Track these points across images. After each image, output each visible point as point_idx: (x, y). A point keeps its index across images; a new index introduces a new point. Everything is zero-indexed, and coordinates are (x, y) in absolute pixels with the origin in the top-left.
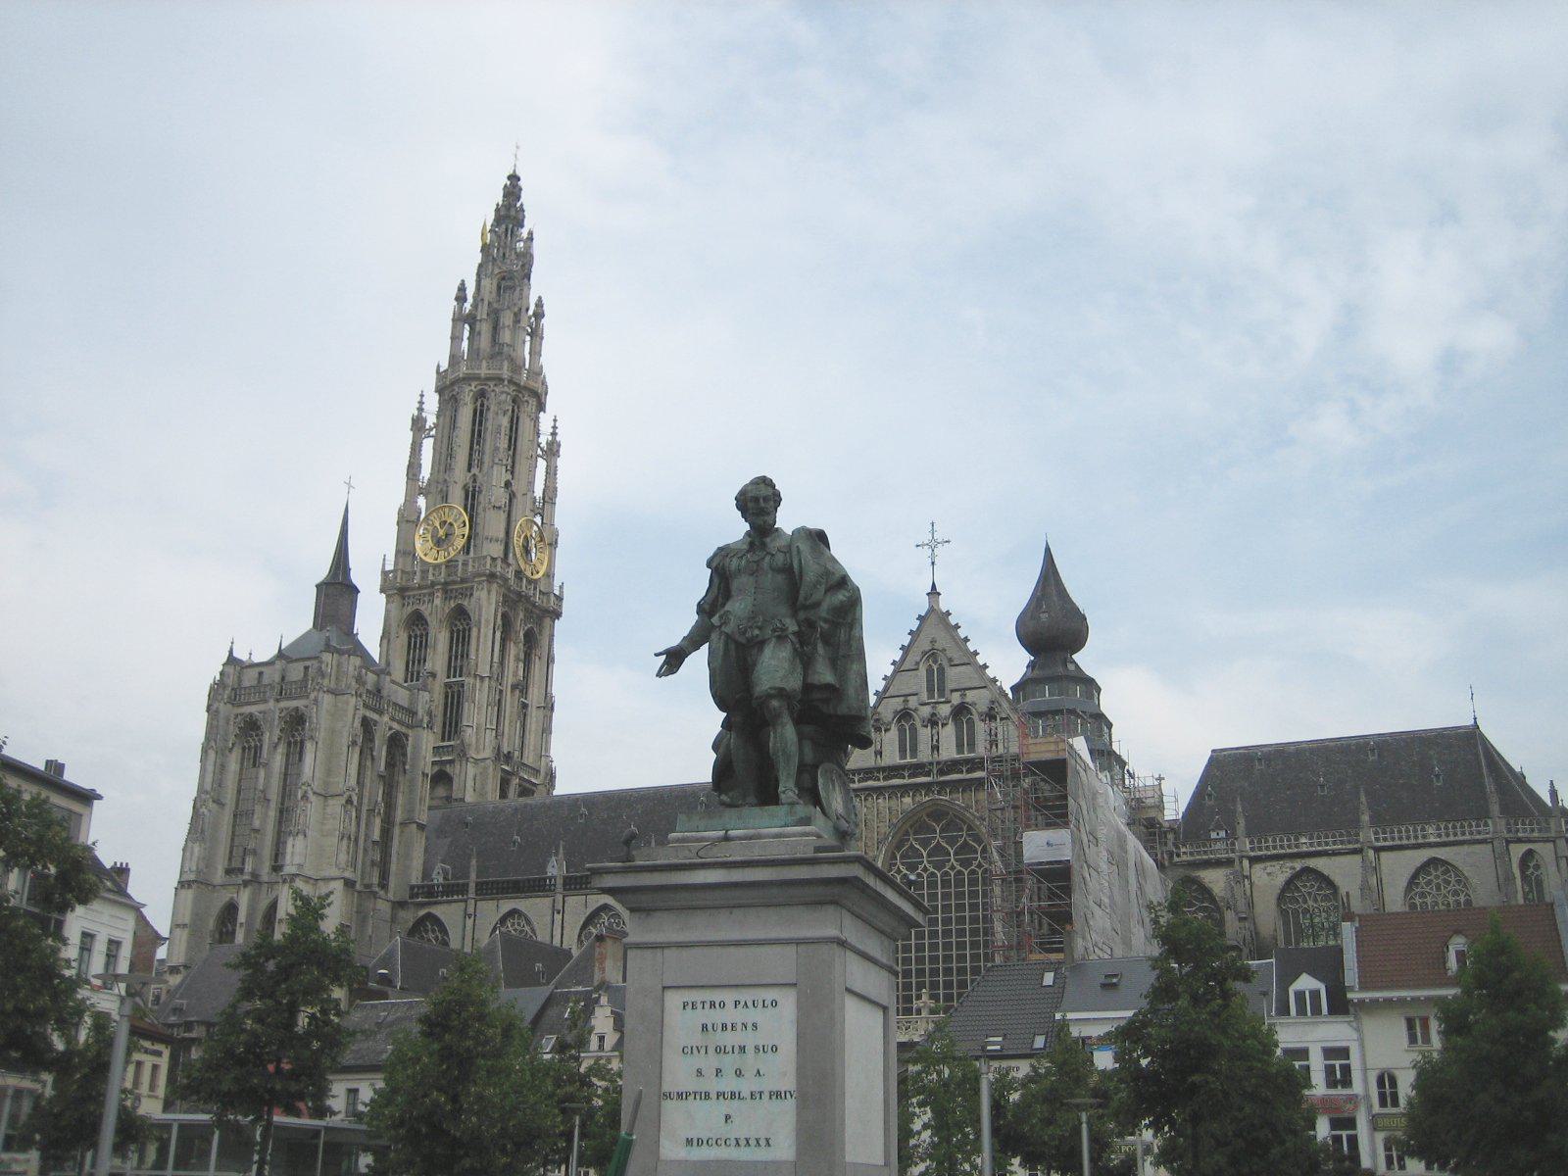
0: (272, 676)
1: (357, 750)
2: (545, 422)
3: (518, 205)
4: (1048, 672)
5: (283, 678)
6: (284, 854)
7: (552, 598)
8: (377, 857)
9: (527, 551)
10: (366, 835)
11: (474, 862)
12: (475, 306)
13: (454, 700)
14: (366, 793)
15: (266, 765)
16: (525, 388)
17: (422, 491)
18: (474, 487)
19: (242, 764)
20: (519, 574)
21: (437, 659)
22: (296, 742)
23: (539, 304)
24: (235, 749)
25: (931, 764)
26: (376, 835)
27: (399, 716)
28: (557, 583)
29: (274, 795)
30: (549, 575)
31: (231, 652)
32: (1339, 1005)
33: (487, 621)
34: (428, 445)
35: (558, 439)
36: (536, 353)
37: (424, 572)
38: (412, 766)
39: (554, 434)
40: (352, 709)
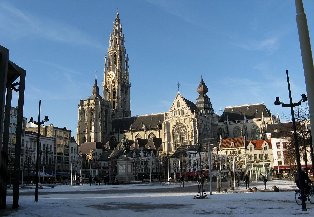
2: (126, 56)
6: (92, 129)
8: (105, 128)
9: (124, 77)
10: (103, 125)
11: (119, 128)
14: (103, 119)
16: (122, 51)
20: (123, 81)
23: (123, 36)
26: (105, 125)
28: (129, 82)
30: (128, 81)
32: (218, 150)
36: (123, 44)
39: (127, 57)
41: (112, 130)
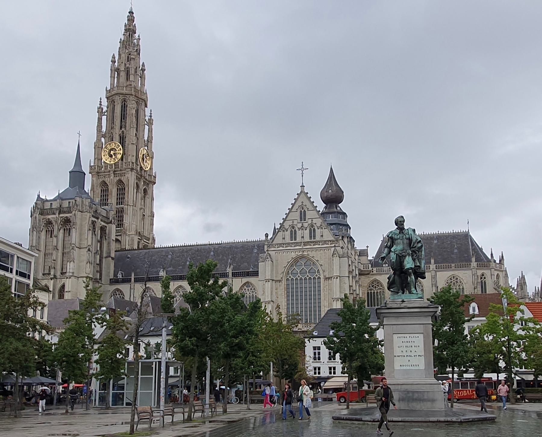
0: (55, 205)
1: (91, 232)
3: (134, 24)
4: (332, 210)
5: (61, 206)
7: (153, 177)
8: (99, 269)
10: (94, 262)
12: (119, 65)
13: (120, 214)
15: (56, 237)
17: (104, 136)
18: (123, 136)
19: (46, 237)
20: (141, 167)
21: (113, 199)
22: (67, 229)
23: (143, 65)
24: (43, 231)
25: (301, 242)
26: (98, 262)
27: (103, 219)
28: (154, 172)
29: (60, 247)
30: (151, 169)
31: (39, 196)
33: (131, 185)
34: (104, 118)
35: (152, 118)
36: (143, 85)
37: (106, 167)
38: (109, 237)
39: (151, 116)
40: (88, 217)
41: (115, 275)
